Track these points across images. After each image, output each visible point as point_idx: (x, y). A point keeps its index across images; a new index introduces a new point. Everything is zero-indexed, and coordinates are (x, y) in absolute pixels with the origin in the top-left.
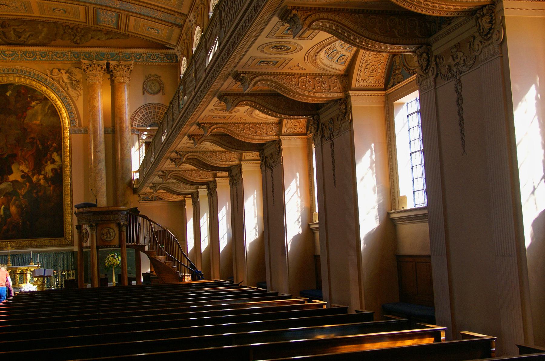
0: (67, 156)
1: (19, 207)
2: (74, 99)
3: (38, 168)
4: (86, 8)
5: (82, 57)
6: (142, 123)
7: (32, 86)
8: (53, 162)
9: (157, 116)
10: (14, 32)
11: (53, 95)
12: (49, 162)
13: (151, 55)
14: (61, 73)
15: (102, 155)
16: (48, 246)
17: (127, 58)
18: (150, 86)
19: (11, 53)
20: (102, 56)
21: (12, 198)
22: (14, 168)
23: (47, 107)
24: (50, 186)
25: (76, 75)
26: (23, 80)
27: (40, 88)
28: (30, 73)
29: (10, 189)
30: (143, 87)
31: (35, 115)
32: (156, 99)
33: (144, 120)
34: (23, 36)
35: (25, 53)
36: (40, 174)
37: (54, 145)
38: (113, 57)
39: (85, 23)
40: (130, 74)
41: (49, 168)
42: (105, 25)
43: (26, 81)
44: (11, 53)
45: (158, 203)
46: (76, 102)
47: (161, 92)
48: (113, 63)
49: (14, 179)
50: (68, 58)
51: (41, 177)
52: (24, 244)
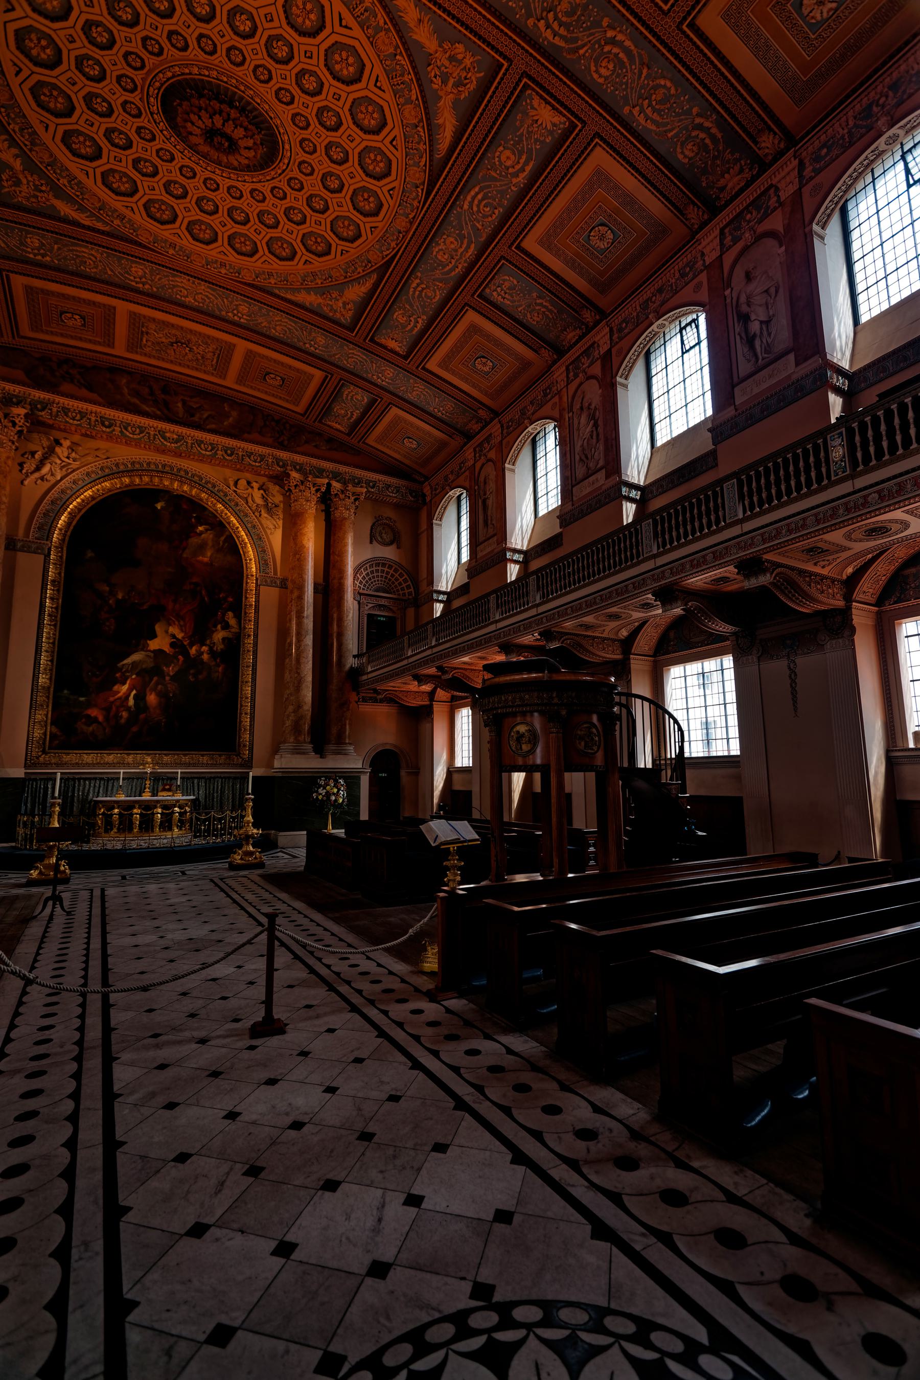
0: (250, 621)
1: (162, 695)
2: (269, 532)
3: (200, 635)
4: (327, 377)
5: (289, 468)
6: (365, 586)
7: (201, 500)
8: (226, 626)
9: (386, 578)
10: (184, 403)
11: (232, 519)
12: (219, 627)
13: (389, 486)
14: (252, 487)
15: (309, 623)
16: (207, 766)
17: (358, 482)
18: (381, 534)
19: (175, 437)
20: (320, 472)
21: (151, 680)
22: (158, 628)
23: (223, 538)
24: (219, 666)
25: (274, 496)
26: (185, 488)
27: (214, 505)
28: (201, 479)
29: (150, 664)
30: (371, 532)
31: (202, 547)
32: (389, 553)
33: (367, 582)
34: (198, 415)
35: (200, 442)
36: (203, 644)
37: (230, 599)
38: (336, 476)
39: (301, 415)
40: (357, 507)
41: (219, 635)
42: (333, 424)
43: (191, 491)
44: (175, 437)
45: (382, 710)
46: (270, 537)
47: (394, 546)
48: (336, 485)
49: (157, 647)
50: (267, 465)
51: (204, 648)
52: (166, 759)
